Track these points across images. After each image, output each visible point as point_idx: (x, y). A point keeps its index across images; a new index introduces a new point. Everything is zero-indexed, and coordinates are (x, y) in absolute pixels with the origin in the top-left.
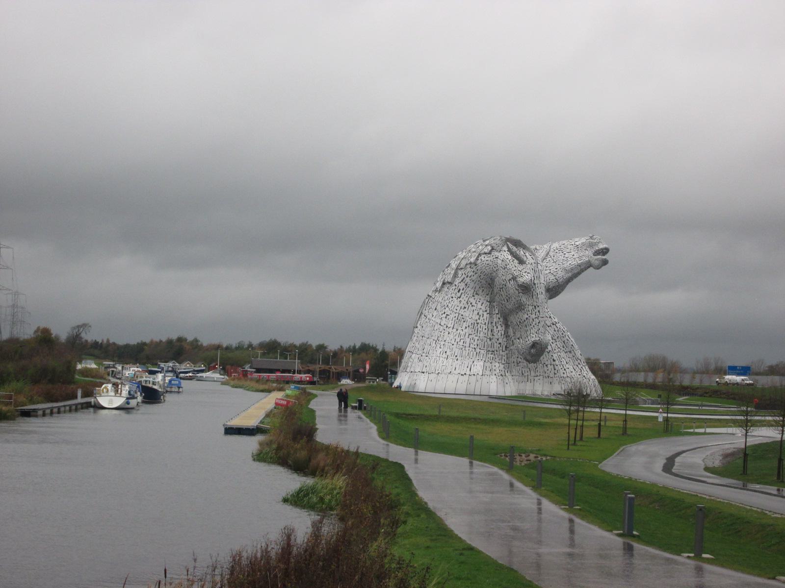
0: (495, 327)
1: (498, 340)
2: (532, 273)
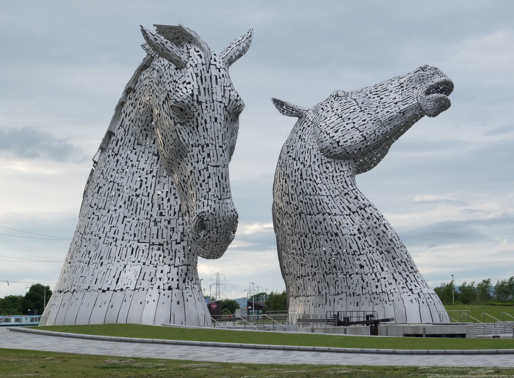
0: (166, 200)
1: (169, 222)
2: (194, 83)
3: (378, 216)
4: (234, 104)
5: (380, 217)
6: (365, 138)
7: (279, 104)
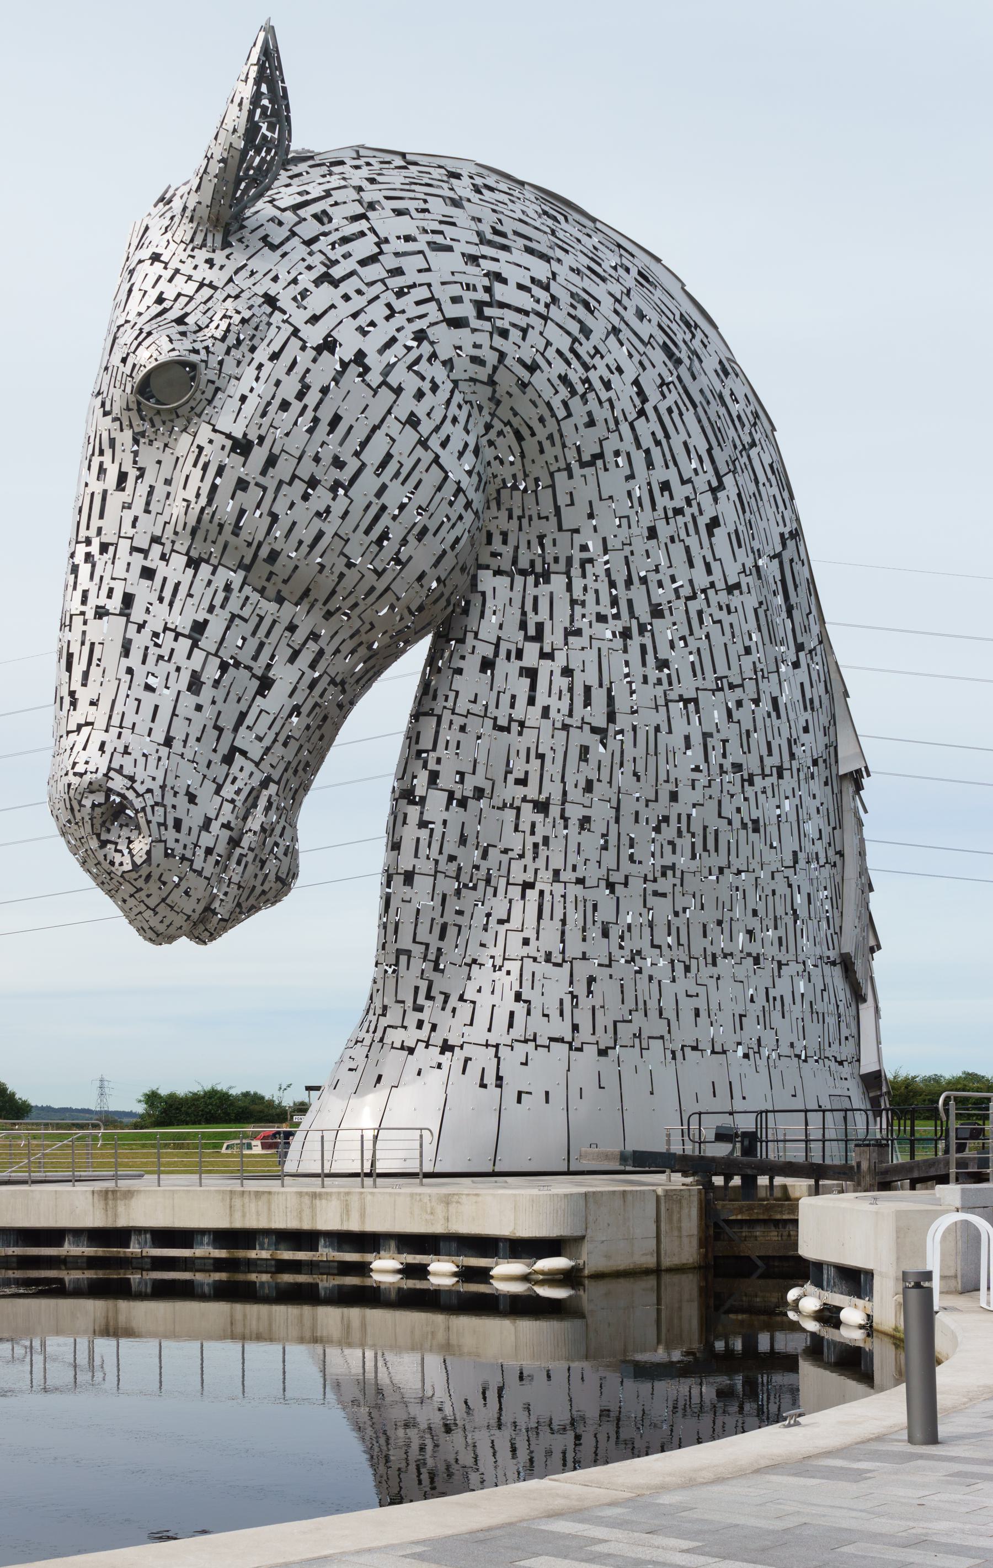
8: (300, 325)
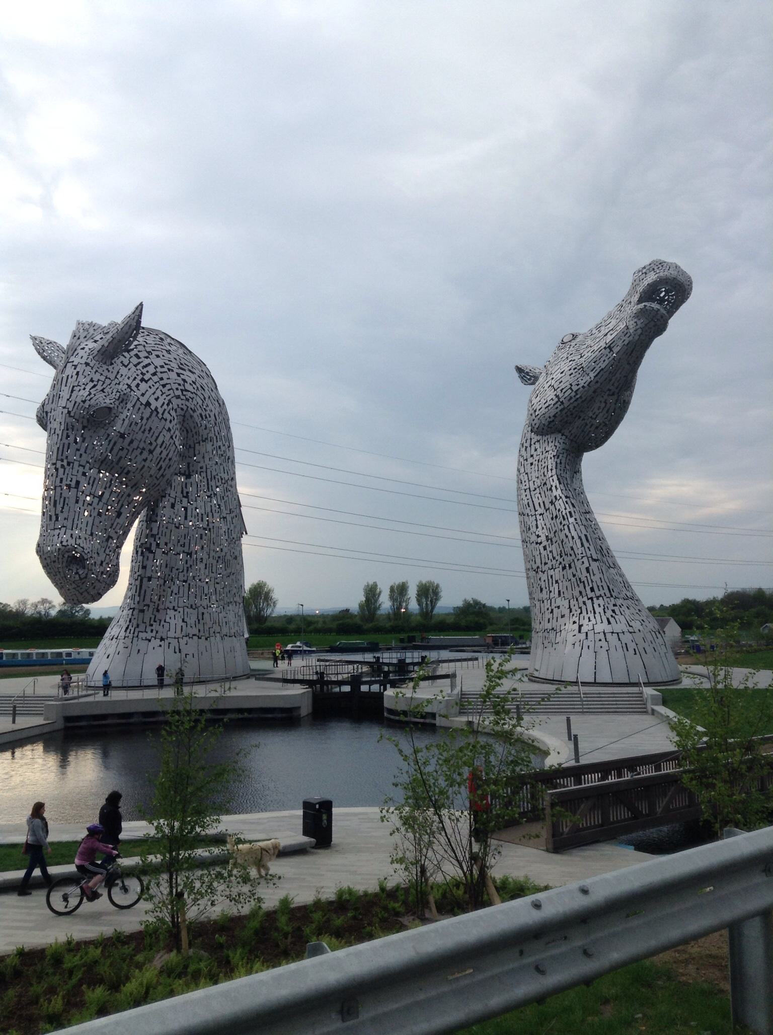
3: (564, 513)
4: (80, 407)
5: (566, 514)
6: (559, 399)
7: (519, 370)
8: (140, 397)
